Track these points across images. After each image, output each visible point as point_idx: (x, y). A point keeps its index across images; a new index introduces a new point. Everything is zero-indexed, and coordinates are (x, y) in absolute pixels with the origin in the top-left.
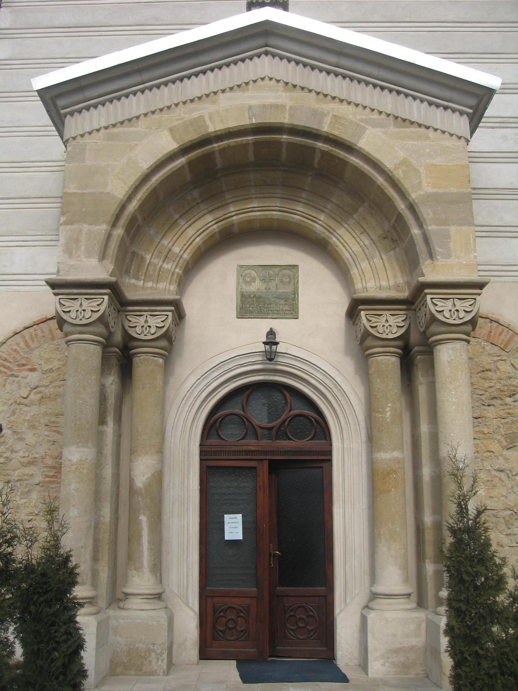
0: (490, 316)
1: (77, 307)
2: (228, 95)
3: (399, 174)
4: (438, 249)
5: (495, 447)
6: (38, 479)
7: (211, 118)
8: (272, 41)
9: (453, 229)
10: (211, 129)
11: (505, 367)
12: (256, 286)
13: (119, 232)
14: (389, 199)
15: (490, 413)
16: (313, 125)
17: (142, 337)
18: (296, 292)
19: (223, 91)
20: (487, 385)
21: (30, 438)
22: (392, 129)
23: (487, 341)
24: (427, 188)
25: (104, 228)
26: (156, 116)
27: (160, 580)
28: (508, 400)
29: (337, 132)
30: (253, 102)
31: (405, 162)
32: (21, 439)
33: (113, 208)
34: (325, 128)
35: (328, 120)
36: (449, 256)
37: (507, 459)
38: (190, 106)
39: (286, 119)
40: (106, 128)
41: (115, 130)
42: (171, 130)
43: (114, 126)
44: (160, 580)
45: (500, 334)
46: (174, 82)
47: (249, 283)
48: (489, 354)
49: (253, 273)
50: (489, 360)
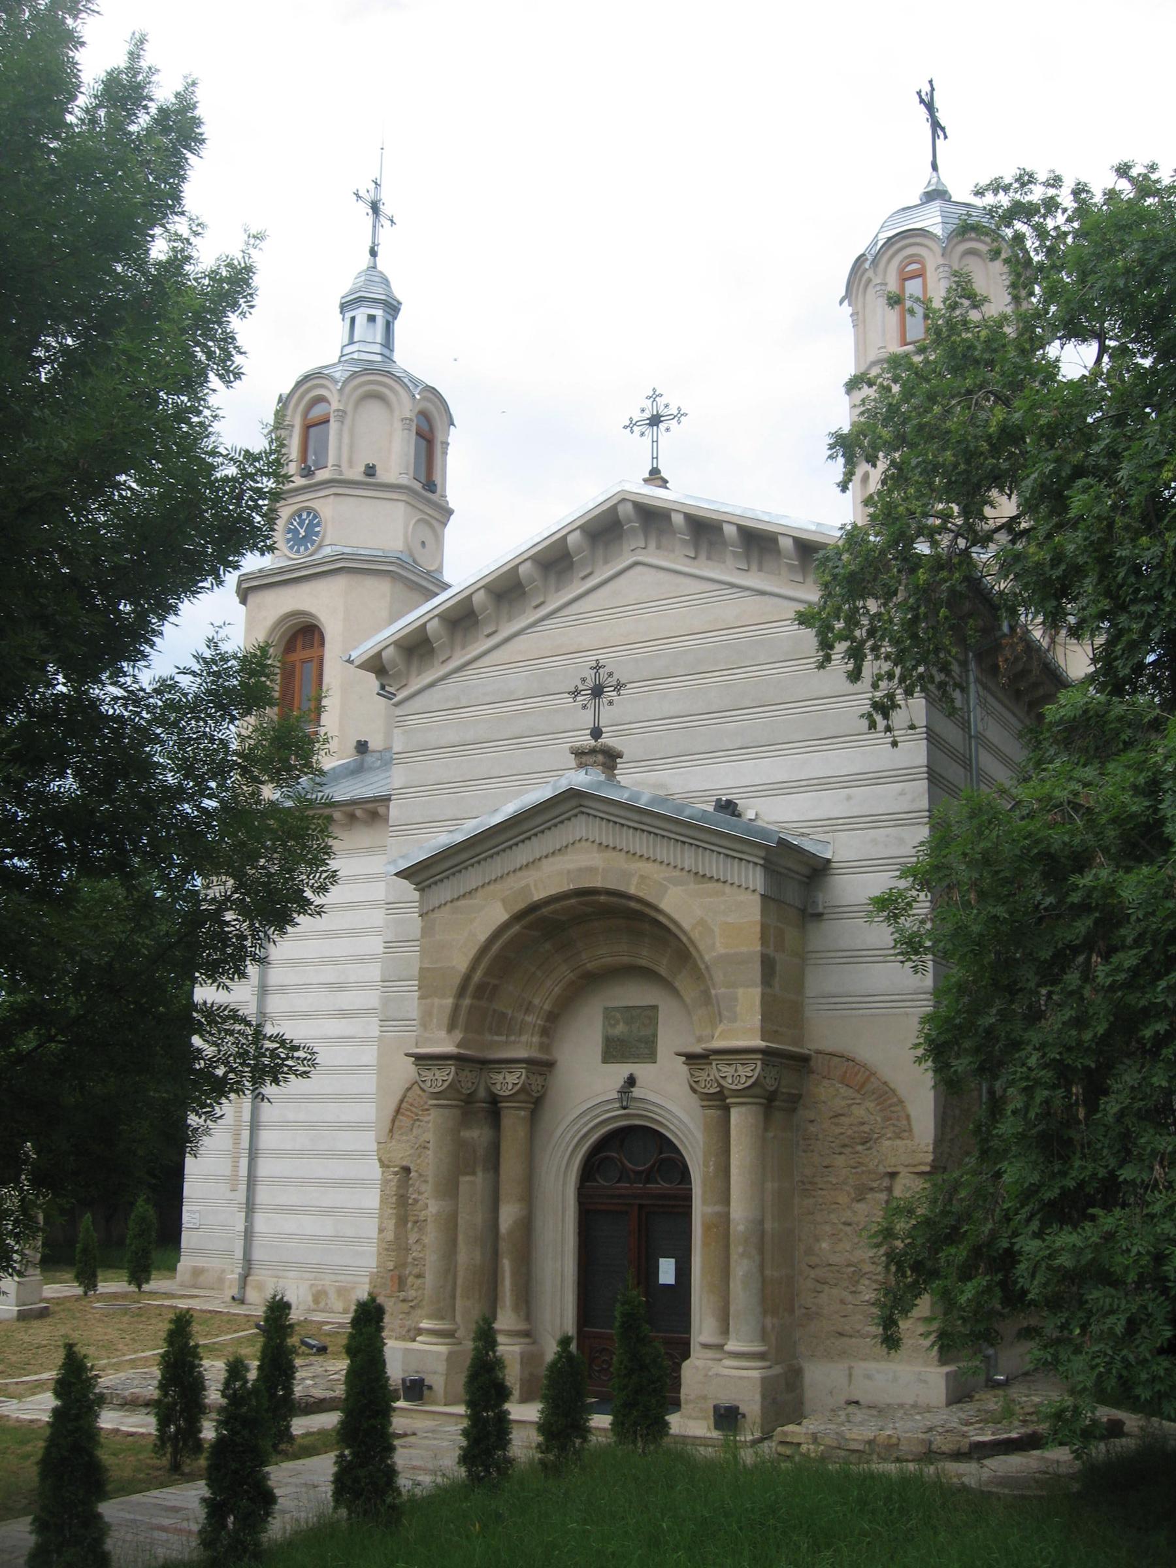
0: (846, 1054)
1: (431, 1077)
2: (551, 860)
3: (695, 935)
4: (725, 1013)
5: (843, 1199)
7: (535, 885)
8: (586, 803)
9: (740, 991)
10: (536, 898)
11: (858, 1111)
12: (620, 1029)
13: (467, 1002)
15: (840, 1161)
16: (622, 888)
17: (501, 1093)
18: (655, 1035)
19: (546, 857)
20: (838, 1130)
22: (692, 886)
23: (842, 1083)
24: (721, 950)
25: (449, 1001)
26: (492, 887)
27: (528, 1318)
28: (860, 1148)
29: (641, 894)
30: (571, 866)
31: (702, 922)
33: (457, 981)
34: (632, 890)
35: (635, 880)
36: (734, 1019)
37: (855, 1212)
38: (519, 874)
39: (598, 883)
40: (452, 901)
42: (503, 901)
43: (458, 899)
44: (528, 1318)
45: (856, 1074)
46: (504, 850)
47: (613, 1026)
48: (844, 1098)
49: (618, 1015)
50: (843, 1103)
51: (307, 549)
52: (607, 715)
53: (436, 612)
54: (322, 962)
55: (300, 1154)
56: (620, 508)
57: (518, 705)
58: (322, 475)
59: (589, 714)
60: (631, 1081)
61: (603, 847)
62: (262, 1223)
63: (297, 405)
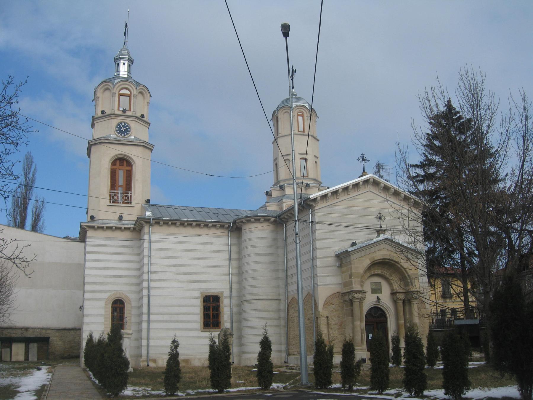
6: (337, 328)
12: (374, 287)
14: (404, 273)
18: (381, 288)
21: (335, 319)
32: (333, 319)
35: (395, 258)
39: (388, 257)
41: (360, 259)
42: (369, 259)
51: (125, 135)
52: (382, 223)
53: (332, 191)
54: (170, 265)
55: (166, 322)
56: (371, 179)
57: (344, 216)
58: (128, 113)
59: (379, 223)
60: (378, 297)
61: (389, 250)
62: (152, 342)
63: (118, 87)
